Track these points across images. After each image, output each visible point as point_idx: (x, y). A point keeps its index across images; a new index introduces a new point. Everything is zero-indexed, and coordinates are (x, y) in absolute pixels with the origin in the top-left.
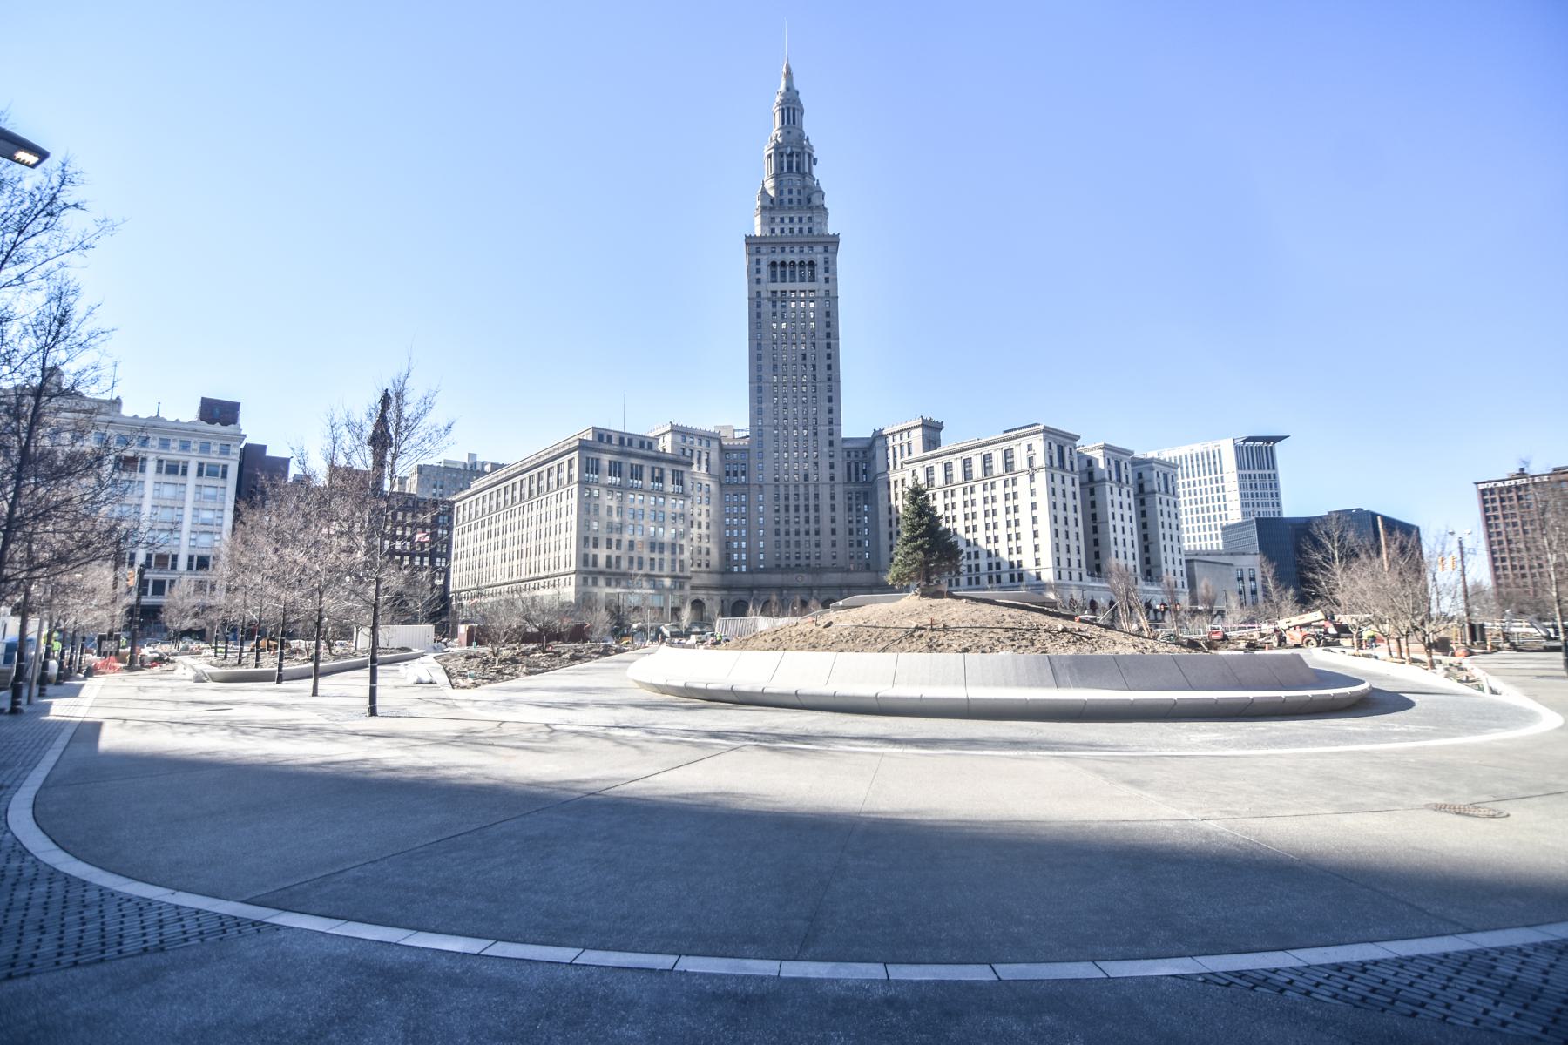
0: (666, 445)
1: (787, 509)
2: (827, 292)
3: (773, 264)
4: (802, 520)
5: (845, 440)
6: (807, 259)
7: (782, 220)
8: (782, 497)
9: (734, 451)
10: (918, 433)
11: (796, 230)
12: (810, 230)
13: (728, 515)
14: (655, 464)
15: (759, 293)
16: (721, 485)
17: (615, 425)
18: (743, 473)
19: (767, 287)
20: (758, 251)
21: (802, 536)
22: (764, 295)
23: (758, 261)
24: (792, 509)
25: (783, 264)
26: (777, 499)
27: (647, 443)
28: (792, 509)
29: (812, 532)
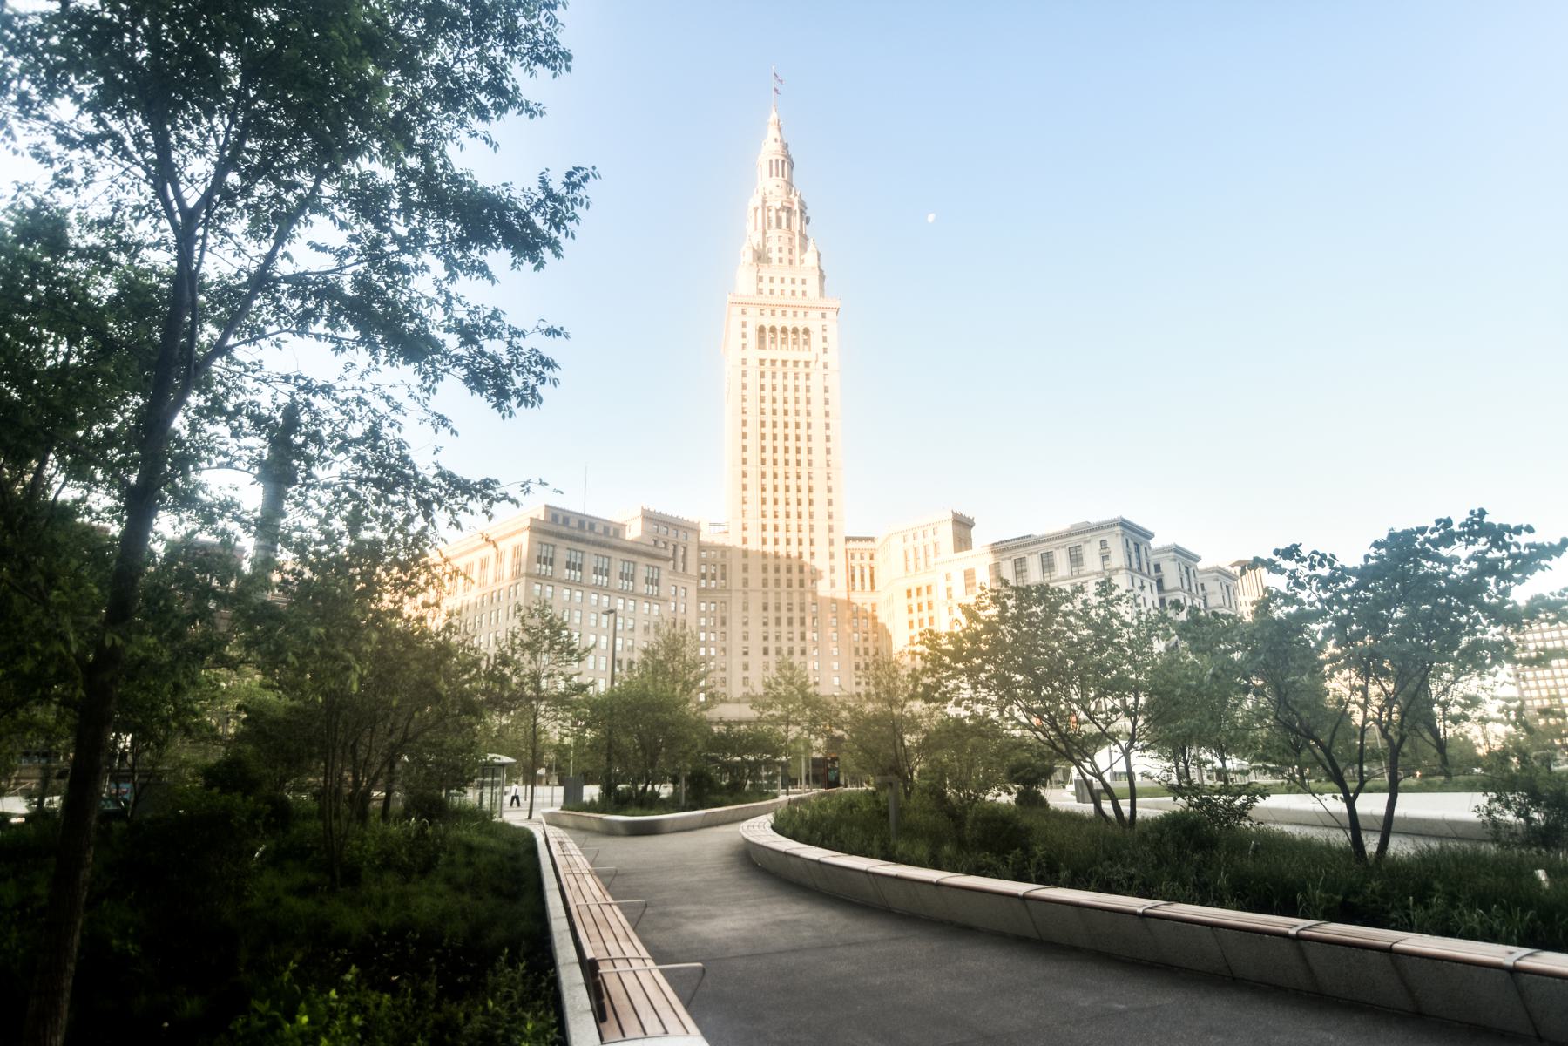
0: (634, 532)
2: (825, 366)
3: (762, 329)
5: (848, 539)
7: (771, 280)
11: (788, 293)
12: (804, 294)
14: (626, 556)
15: (744, 362)
16: (699, 590)
17: (580, 510)
19: (754, 354)
20: (744, 312)
23: (744, 325)
24: (784, 622)
25: (773, 330)
26: (765, 608)
27: (618, 530)
28: (784, 622)
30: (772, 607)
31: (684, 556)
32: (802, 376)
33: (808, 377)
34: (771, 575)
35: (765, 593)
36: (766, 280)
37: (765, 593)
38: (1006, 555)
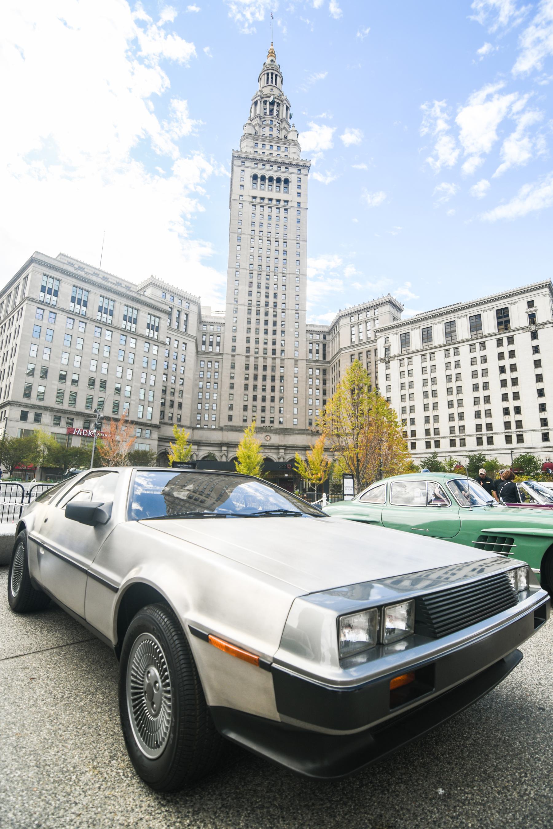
1: (256, 377)
3: (255, 177)
4: (268, 388)
6: (283, 177)
8: (252, 367)
9: (212, 324)
10: (388, 308)
13: (201, 379)
14: (130, 303)
16: (197, 352)
18: (218, 344)
21: (268, 404)
22: (246, 198)
24: (260, 378)
25: (263, 178)
26: (247, 368)
28: (260, 378)
29: (277, 399)
30: (252, 367)
31: (186, 321)
32: (282, 210)
33: (286, 210)
34: (252, 345)
35: (248, 357)
36: (260, 146)
37: (248, 357)
38: (438, 319)
